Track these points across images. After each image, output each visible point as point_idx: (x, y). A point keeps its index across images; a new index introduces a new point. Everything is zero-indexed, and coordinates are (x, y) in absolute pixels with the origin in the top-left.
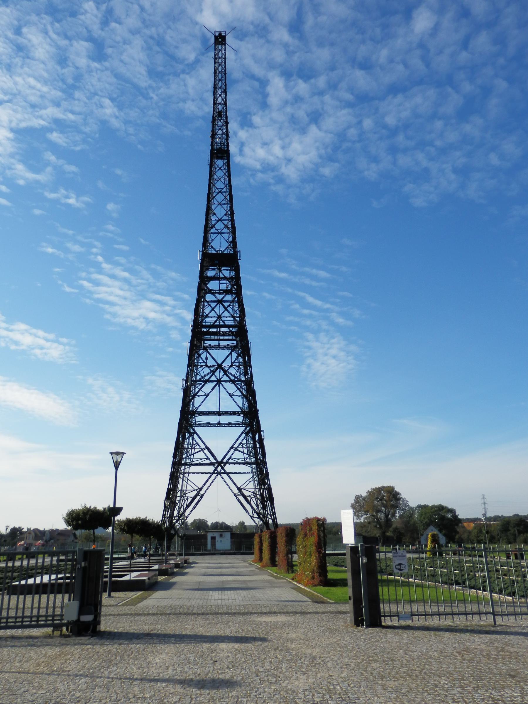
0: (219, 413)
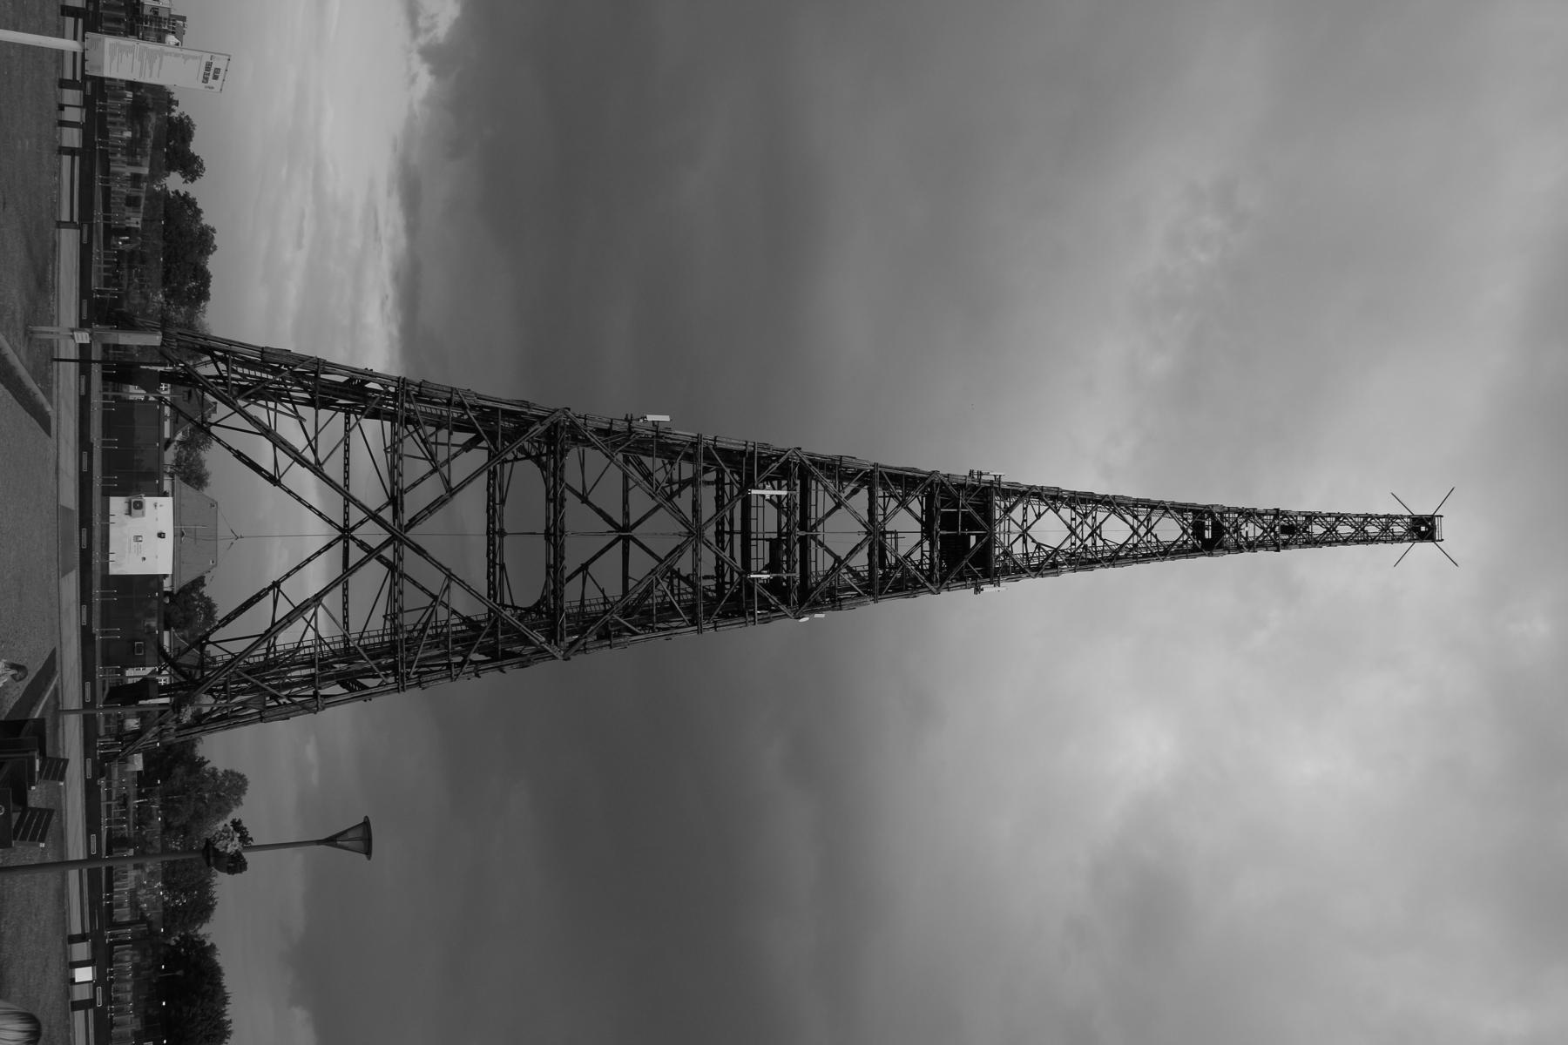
0: (554, 535)
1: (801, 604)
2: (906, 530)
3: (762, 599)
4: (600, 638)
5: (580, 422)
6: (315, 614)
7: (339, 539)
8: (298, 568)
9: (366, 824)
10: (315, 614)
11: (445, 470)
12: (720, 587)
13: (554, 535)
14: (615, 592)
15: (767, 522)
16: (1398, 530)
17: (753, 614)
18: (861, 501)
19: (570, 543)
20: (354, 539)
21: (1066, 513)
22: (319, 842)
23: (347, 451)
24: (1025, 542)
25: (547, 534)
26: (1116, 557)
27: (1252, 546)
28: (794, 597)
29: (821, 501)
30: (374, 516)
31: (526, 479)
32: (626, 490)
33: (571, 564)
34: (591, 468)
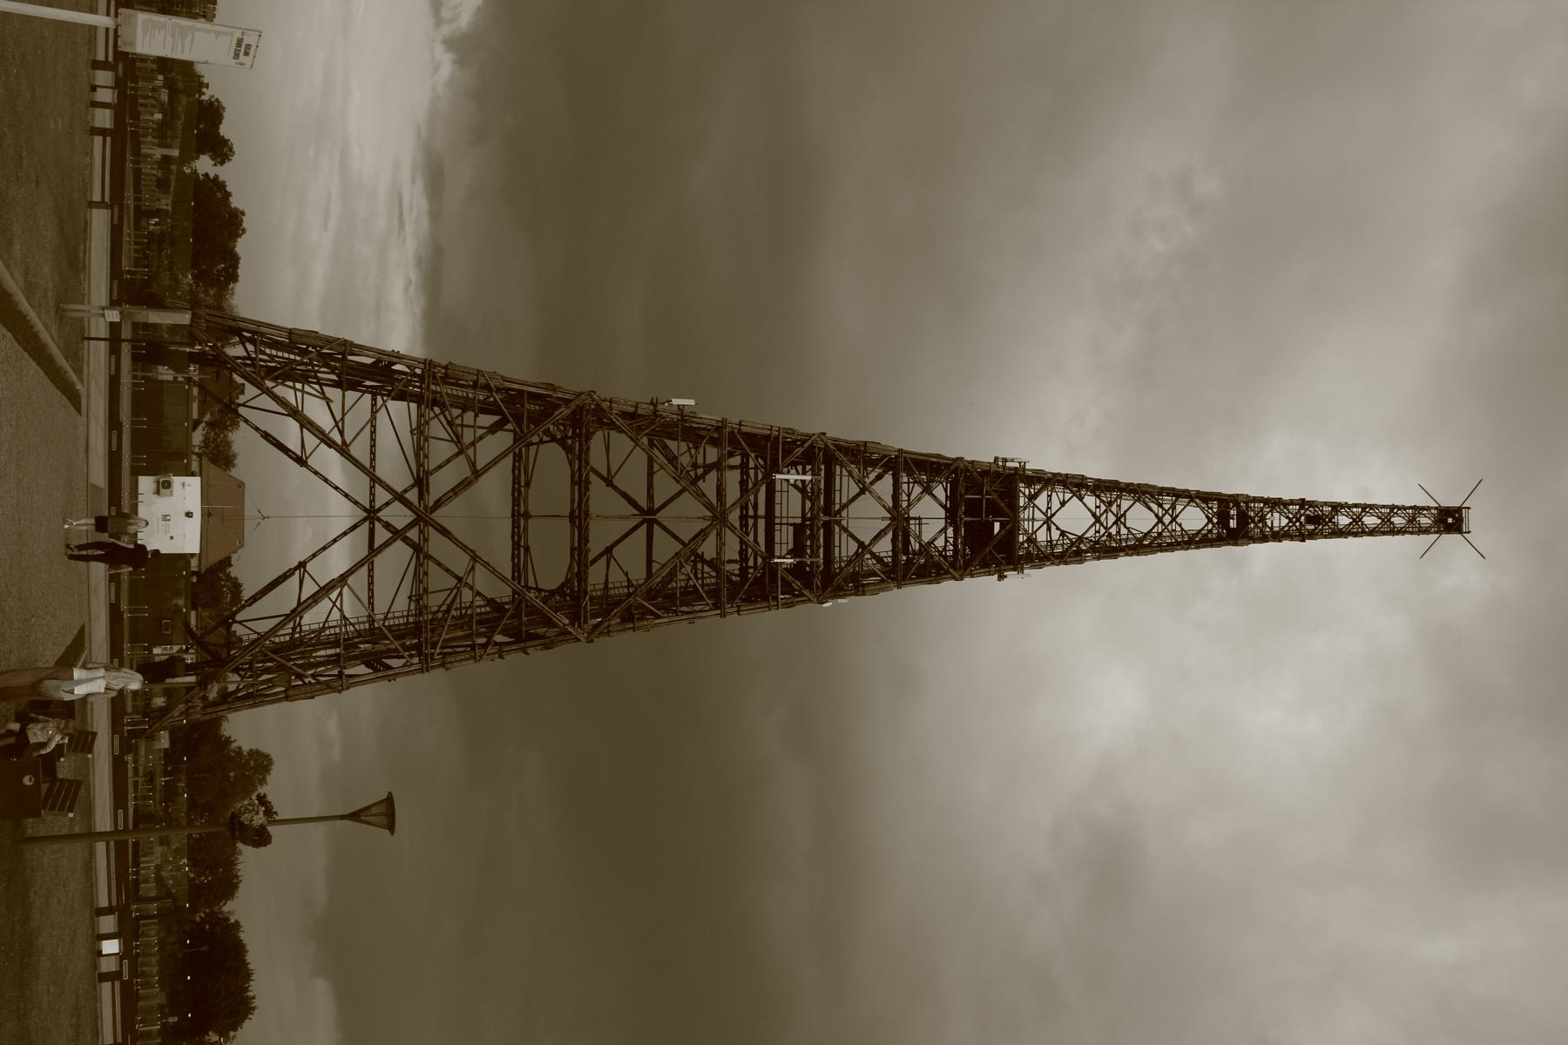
0: (579, 517)
1: (824, 589)
2: (931, 517)
3: (786, 583)
4: (624, 620)
5: (606, 405)
6: (340, 594)
7: (364, 520)
8: (324, 548)
9: (389, 800)
10: (340, 594)
11: (470, 452)
12: (744, 571)
13: (579, 517)
14: (638, 574)
15: (791, 507)
16: (1425, 521)
17: (776, 598)
18: (885, 487)
19: (595, 527)
20: (379, 520)
21: (1090, 500)
22: (342, 817)
23: (373, 432)
24: (1049, 529)
25: (572, 517)
26: (1141, 546)
27: (1278, 536)
28: (818, 582)
29: (846, 487)
30: (399, 497)
31: (551, 462)
32: (651, 474)
33: (595, 548)
34: (618, 453)
